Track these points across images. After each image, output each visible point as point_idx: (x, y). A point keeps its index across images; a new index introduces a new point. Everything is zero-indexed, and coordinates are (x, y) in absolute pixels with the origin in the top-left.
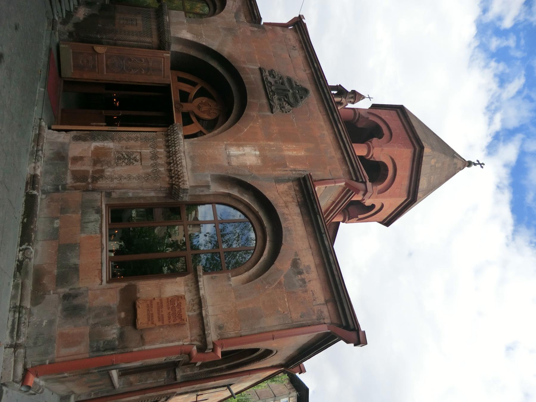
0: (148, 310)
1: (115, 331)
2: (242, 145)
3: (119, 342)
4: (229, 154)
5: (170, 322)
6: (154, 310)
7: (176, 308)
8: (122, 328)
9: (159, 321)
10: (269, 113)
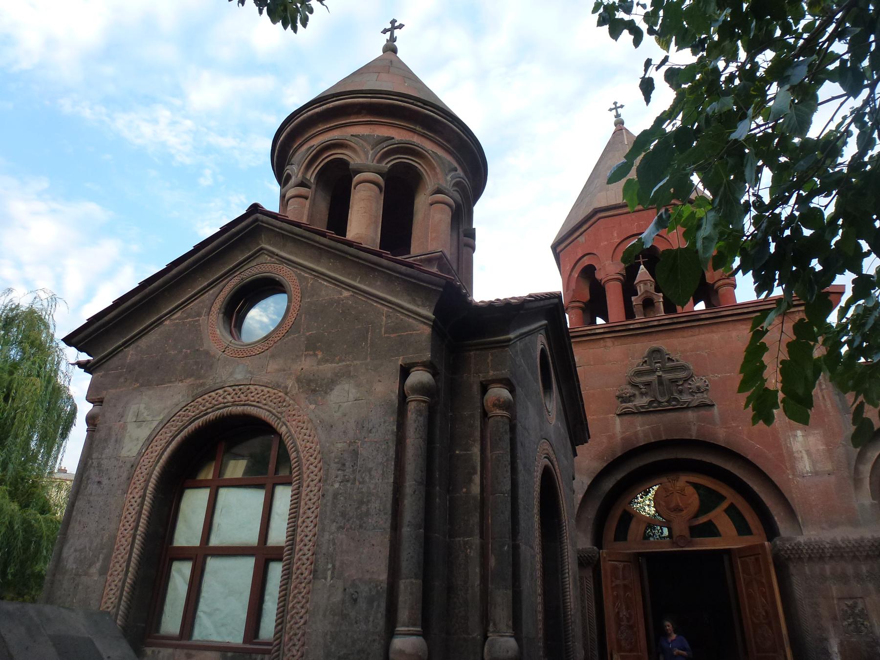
2: (791, 453)
4: (811, 472)
10: (716, 410)
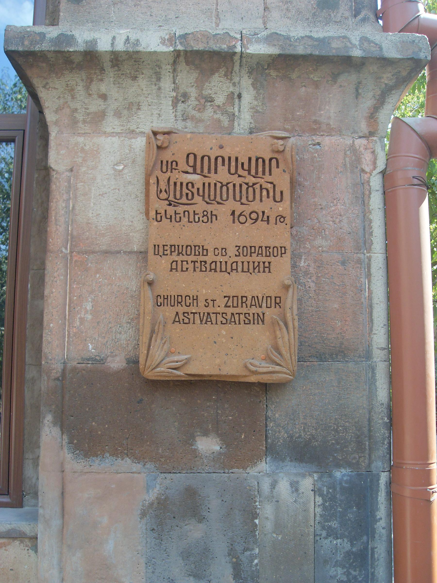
0: (207, 319)
1: (284, 486)
3: (338, 466)
5: (281, 218)
6: (208, 287)
7: (213, 178)
8: (272, 451)
9: (268, 268)
